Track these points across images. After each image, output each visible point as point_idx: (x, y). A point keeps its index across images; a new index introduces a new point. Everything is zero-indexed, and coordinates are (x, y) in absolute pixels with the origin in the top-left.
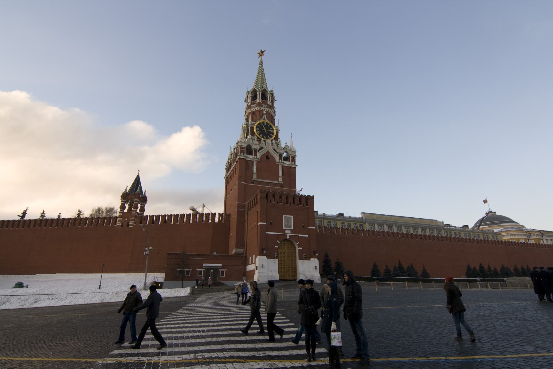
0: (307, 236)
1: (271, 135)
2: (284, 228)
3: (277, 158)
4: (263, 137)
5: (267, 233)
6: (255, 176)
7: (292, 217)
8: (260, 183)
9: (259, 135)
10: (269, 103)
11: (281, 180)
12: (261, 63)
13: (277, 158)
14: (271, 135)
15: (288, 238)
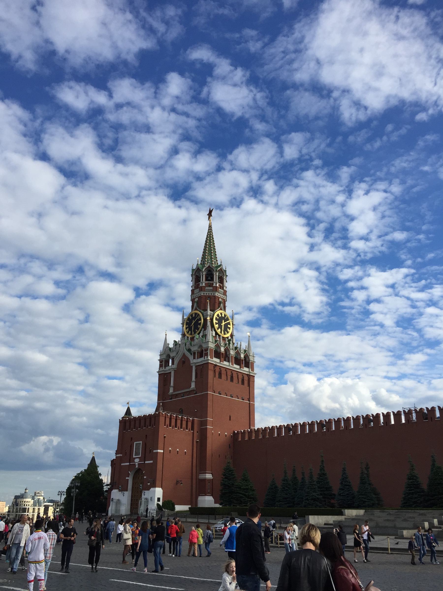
0: (152, 462)
1: (199, 326)
2: (134, 457)
3: (191, 358)
4: (191, 334)
5: (122, 464)
6: (171, 390)
7: (141, 442)
8: (176, 396)
9: (188, 333)
10: (201, 285)
11: (193, 386)
12: (210, 227)
13: (191, 358)
14: (199, 326)
15: (137, 467)
